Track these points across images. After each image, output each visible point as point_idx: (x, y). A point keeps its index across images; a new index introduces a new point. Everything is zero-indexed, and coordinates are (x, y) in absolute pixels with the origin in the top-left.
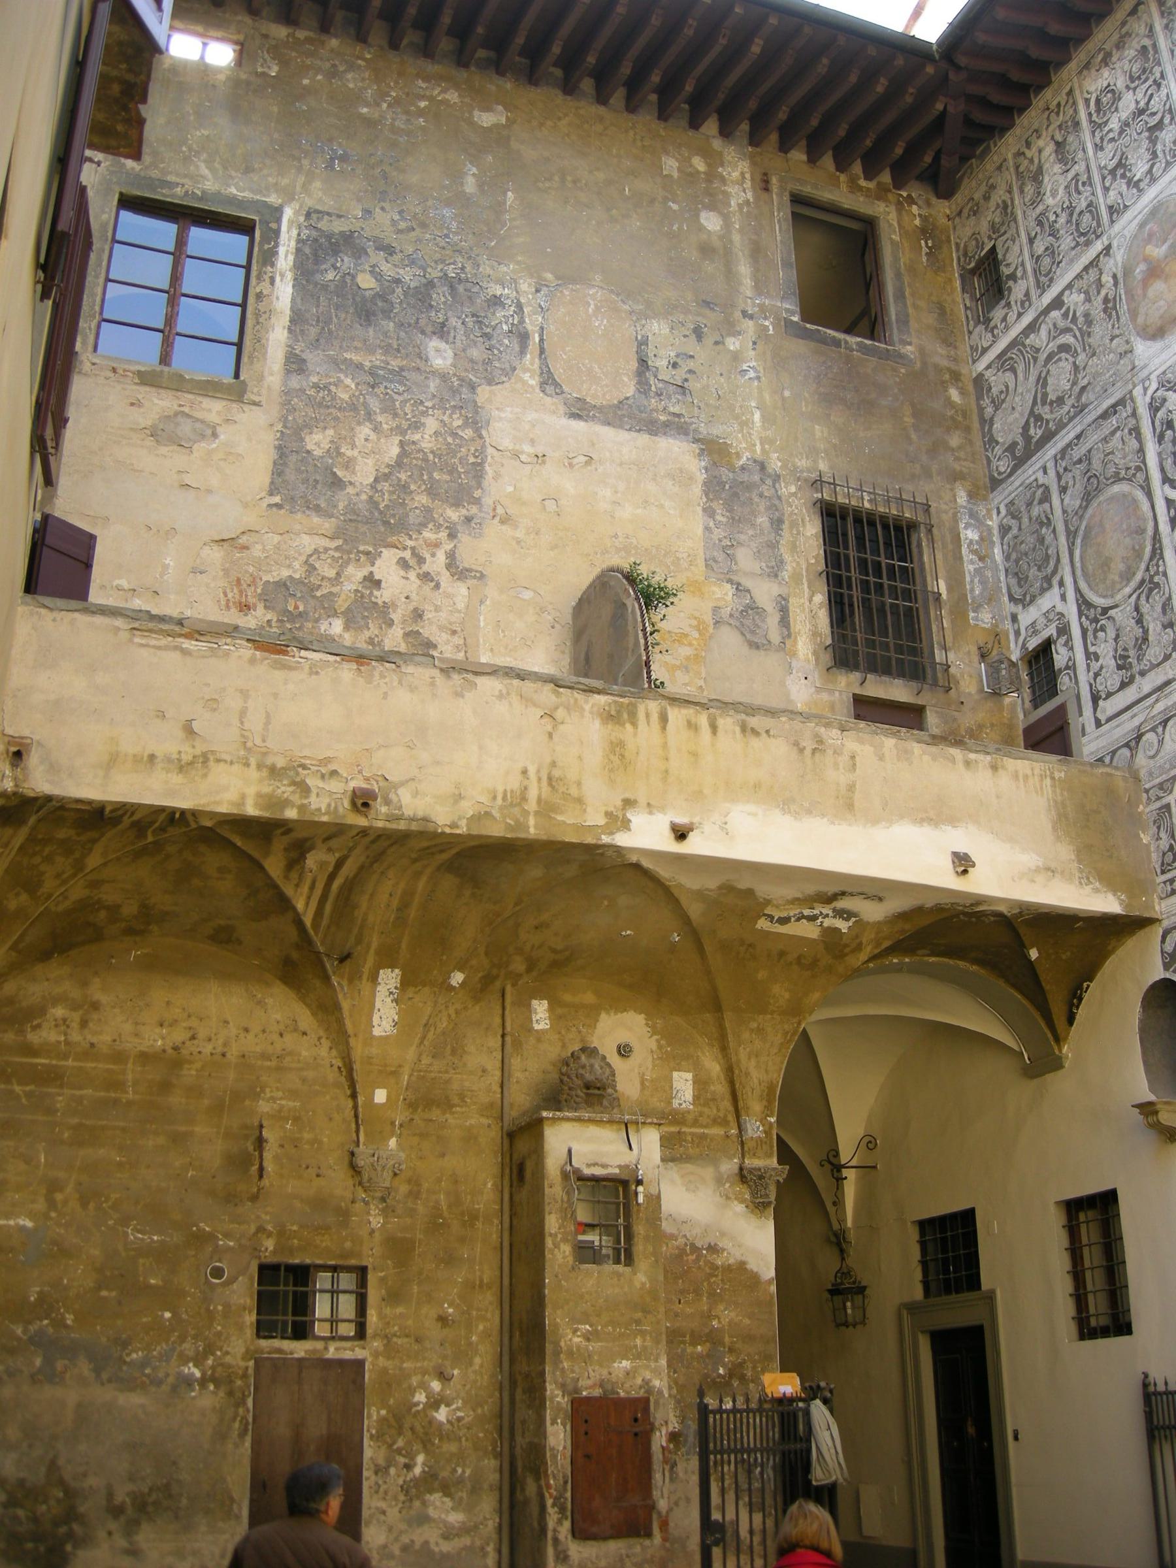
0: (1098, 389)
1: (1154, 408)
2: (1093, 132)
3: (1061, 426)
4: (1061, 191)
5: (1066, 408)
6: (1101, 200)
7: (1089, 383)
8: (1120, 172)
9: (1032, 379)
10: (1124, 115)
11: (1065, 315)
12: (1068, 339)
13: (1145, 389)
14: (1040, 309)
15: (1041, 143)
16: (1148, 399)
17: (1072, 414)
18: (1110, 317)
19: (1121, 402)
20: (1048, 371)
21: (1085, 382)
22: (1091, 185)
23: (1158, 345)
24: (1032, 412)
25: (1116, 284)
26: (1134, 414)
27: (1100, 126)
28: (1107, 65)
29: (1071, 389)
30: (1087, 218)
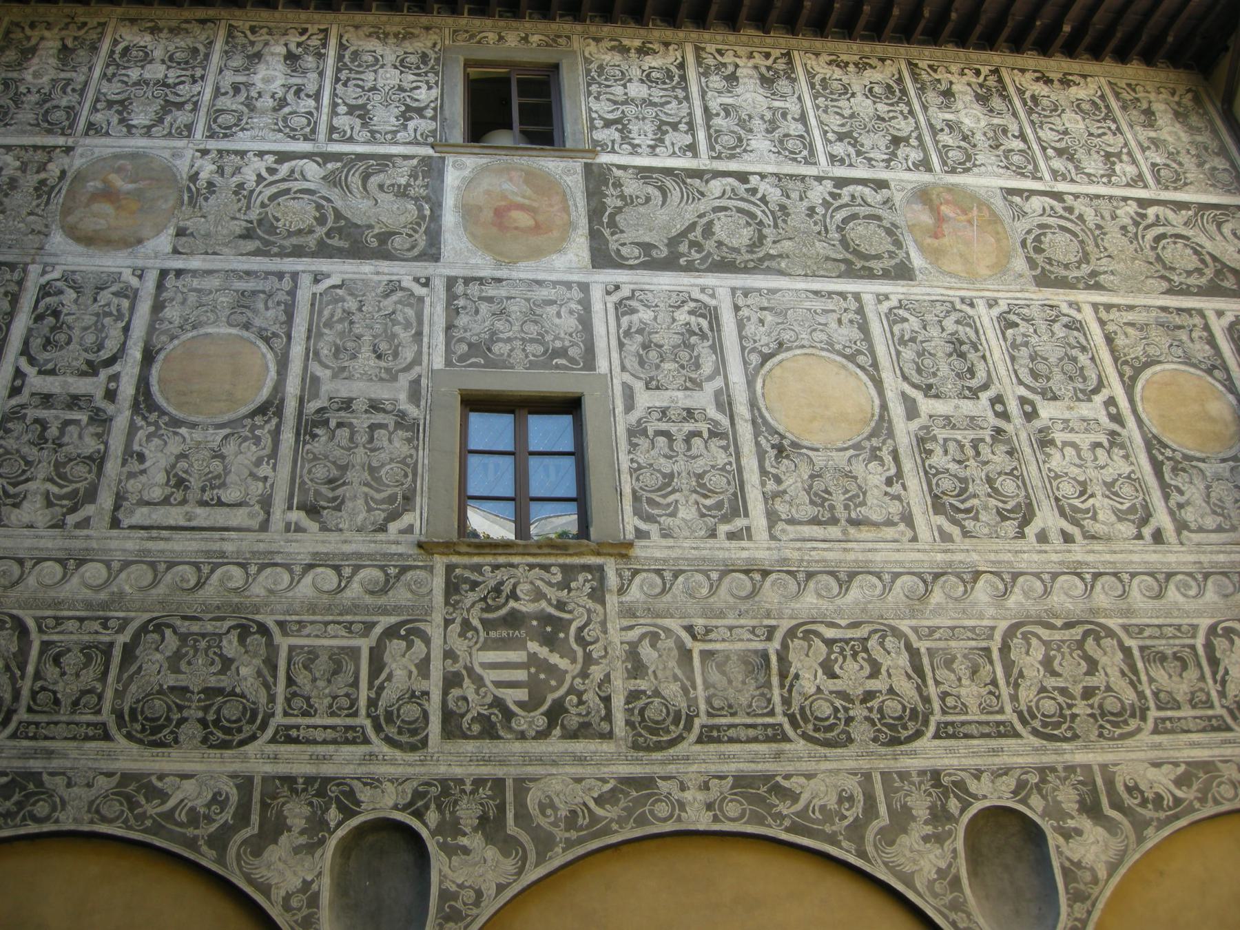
2: (108, 66)
4: (46, 79)
6: (85, 113)
8: (116, 107)
10: (147, 76)
13: (44, 273)
15: (47, 34)
16: (43, 280)
18: (39, 197)
19: (12, 266)
22: (81, 95)
23: (80, 249)
26: (20, 283)
27: (118, 65)
28: (152, 33)
30: (59, 115)
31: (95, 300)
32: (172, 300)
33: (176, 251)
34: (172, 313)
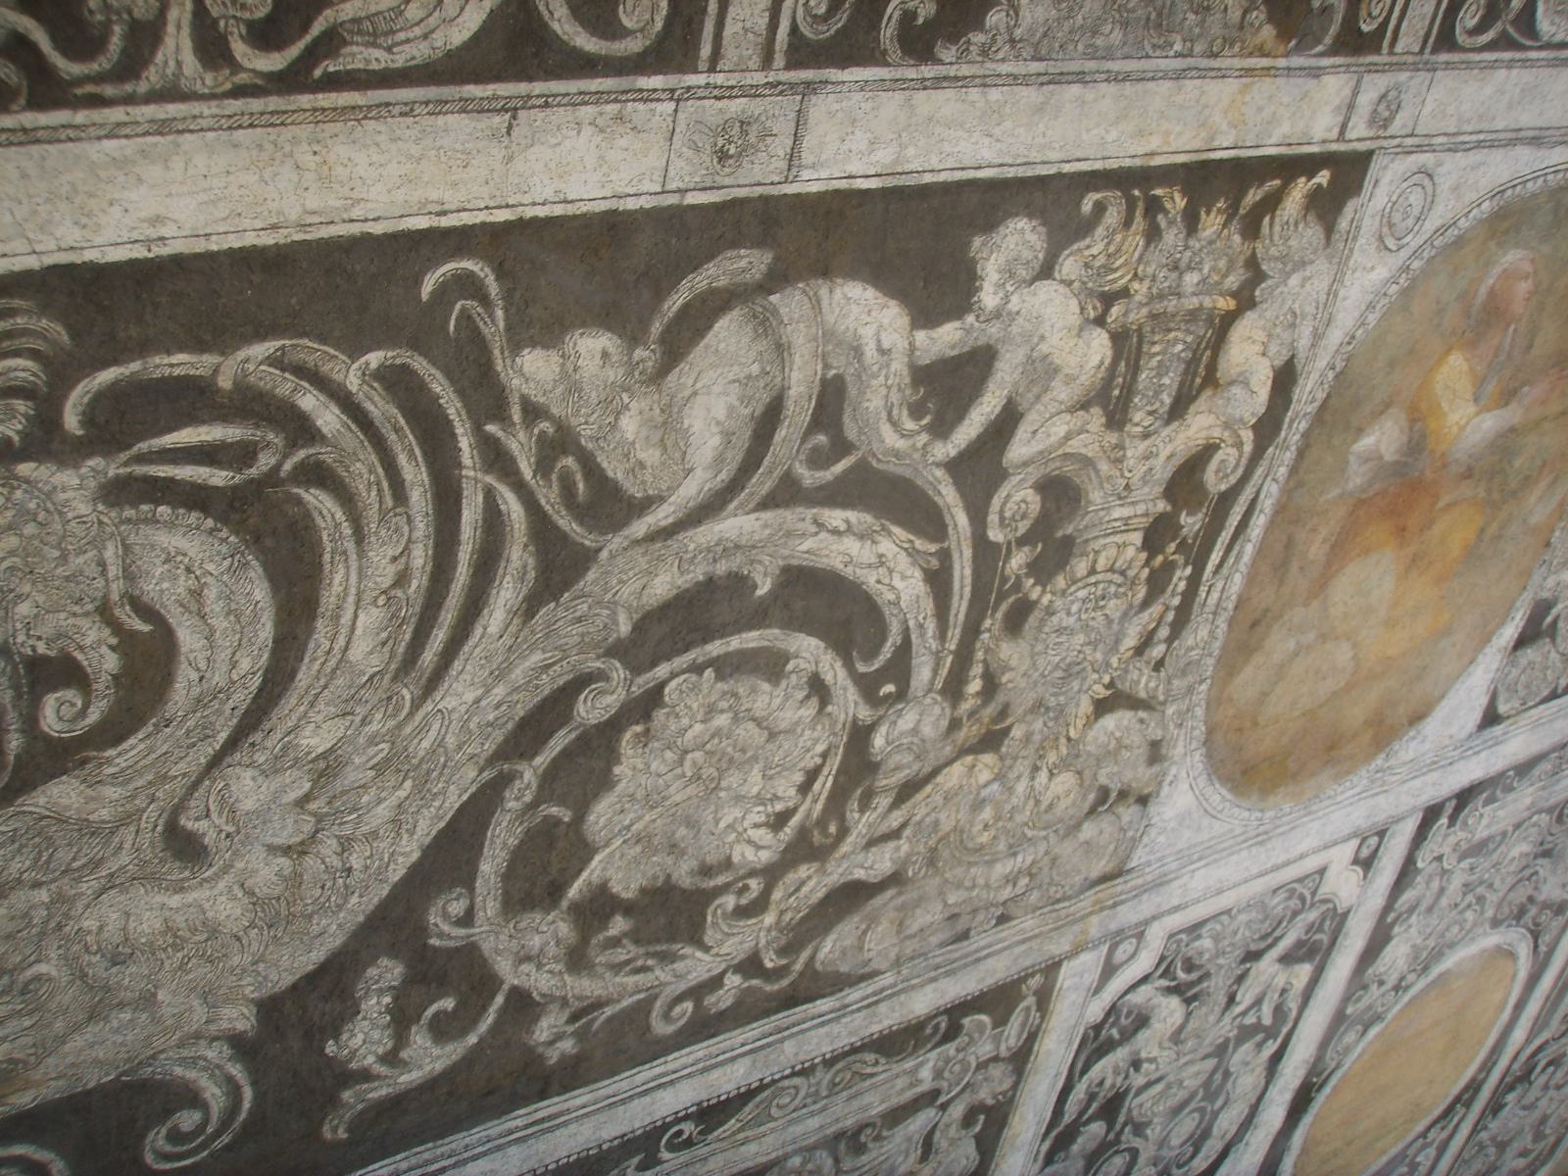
0: (929, 915)
1: (1095, 1044)
3: (621, 1043)
5: (696, 965)
7: (896, 879)
9: (477, 697)
11: (945, 387)
12: (885, 563)
13: (1109, 970)
14: (759, 175)
16: (1096, 1010)
17: (722, 1000)
18: (1157, 583)
19: (998, 1001)
20: (654, 697)
21: (882, 862)
23: (1235, 815)
24: (395, 923)
25: (1267, 428)
26: (1020, 1059)
29: (772, 874)
31: (1231, 1000)
32: (1411, 910)
33: (1491, 718)
34: (1396, 956)
